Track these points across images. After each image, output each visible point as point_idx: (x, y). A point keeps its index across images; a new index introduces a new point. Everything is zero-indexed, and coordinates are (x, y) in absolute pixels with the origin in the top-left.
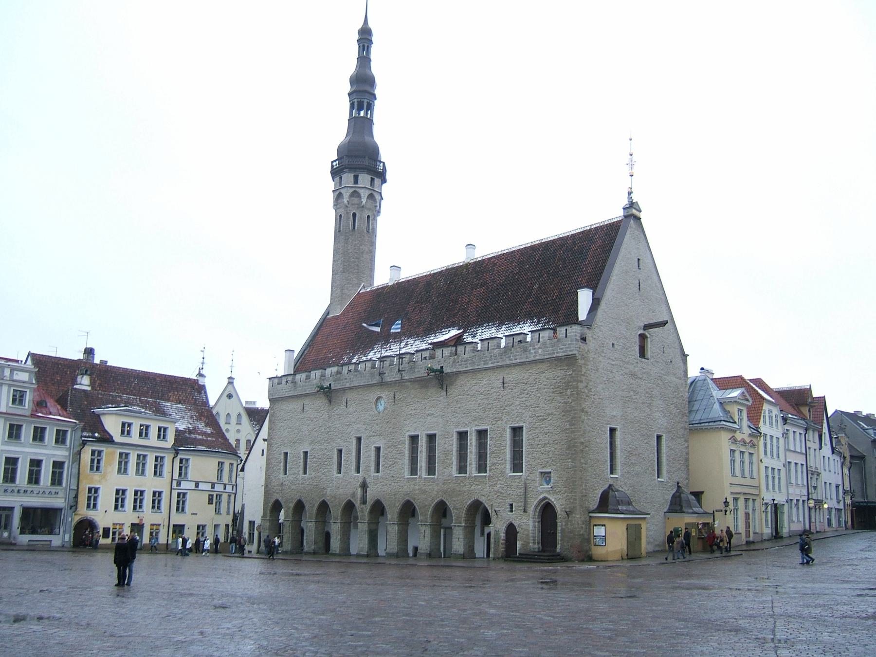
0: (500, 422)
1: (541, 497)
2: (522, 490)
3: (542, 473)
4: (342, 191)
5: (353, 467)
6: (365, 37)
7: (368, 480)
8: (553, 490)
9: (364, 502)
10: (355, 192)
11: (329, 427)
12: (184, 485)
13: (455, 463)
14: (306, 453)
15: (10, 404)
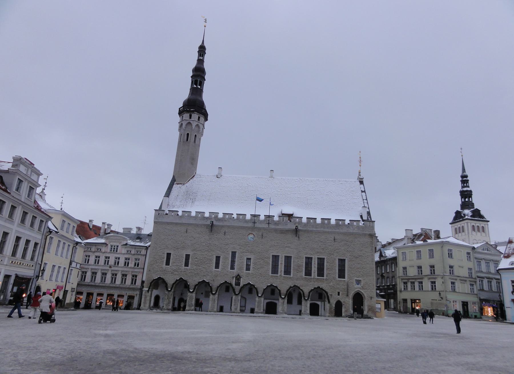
0: (332, 256)
1: (356, 290)
2: (346, 287)
3: (356, 280)
4: (191, 122)
5: (229, 267)
6: (202, 50)
7: (241, 274)
8: (363, 288)
9: (238, 284)
10: (197, 125)
11: (210, 244)
12: (74, 265)
13: (304, 271)
14: (188, 256)
15: (26, 197)
